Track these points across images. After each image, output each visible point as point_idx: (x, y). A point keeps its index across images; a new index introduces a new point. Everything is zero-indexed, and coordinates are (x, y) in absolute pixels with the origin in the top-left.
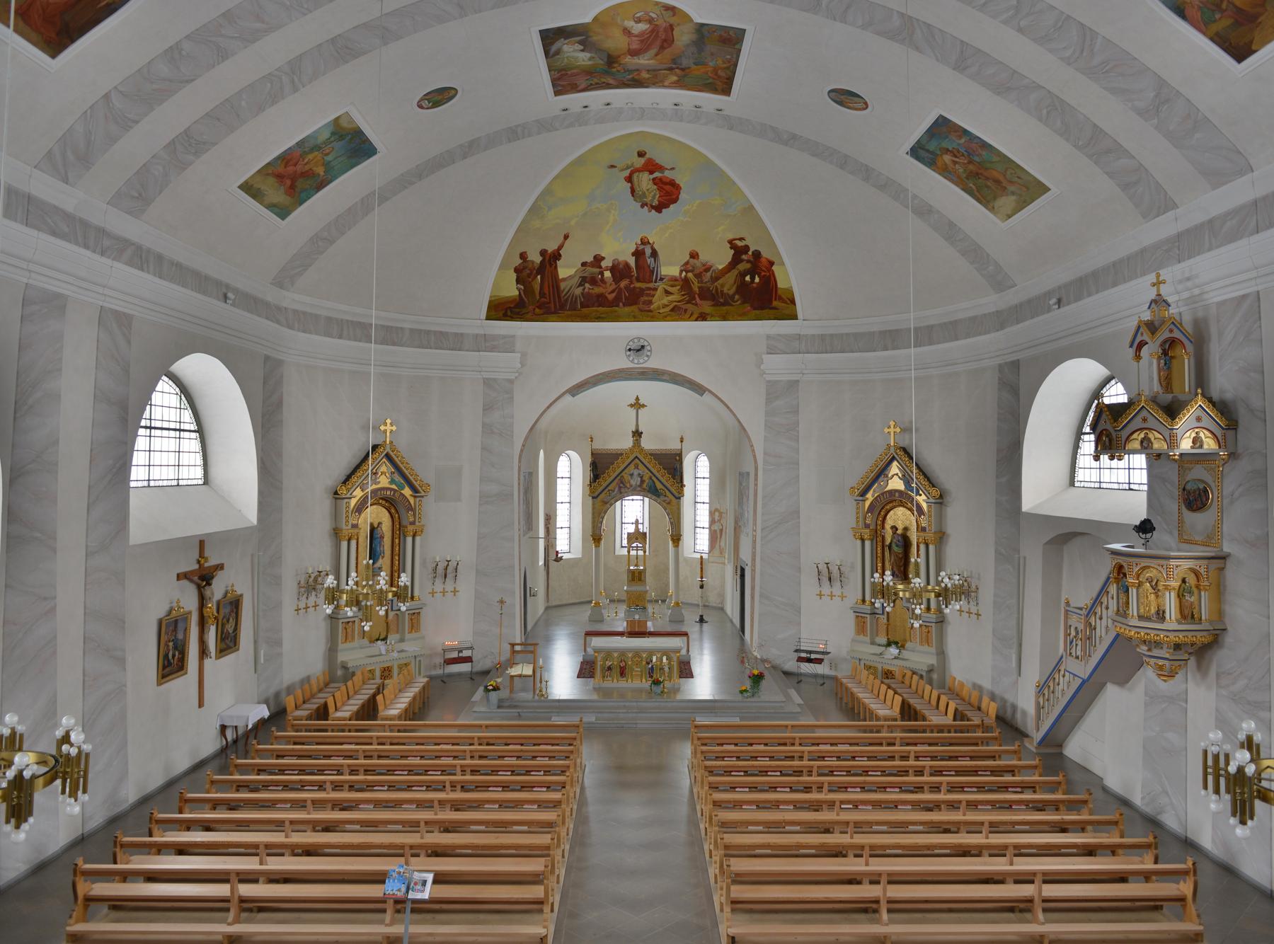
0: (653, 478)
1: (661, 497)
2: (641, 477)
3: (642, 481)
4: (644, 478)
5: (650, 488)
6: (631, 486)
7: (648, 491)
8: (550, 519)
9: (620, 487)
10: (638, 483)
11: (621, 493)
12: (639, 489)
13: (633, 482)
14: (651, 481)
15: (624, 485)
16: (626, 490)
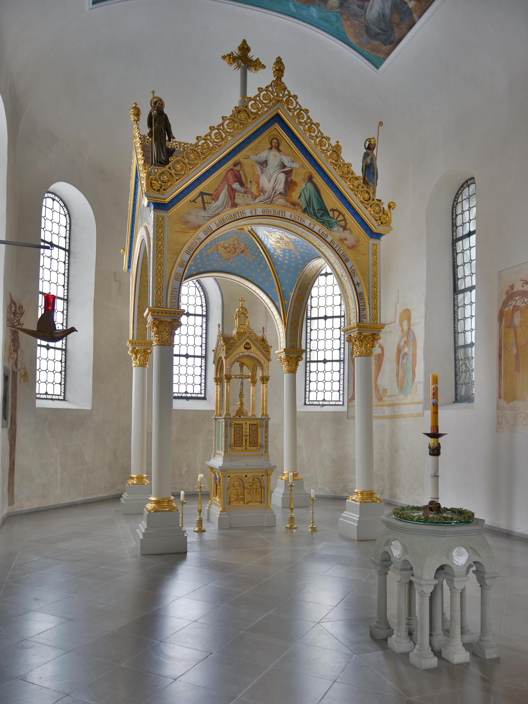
0: (318, 180)
1: (336, 228)
2: (288, 173)
3: (289, 185)
4: (293, 177)
5: (309, 203)
6: (262, 191)
7: (305, 211)
8: (22, 314)
9: (232, 192)
10: (280, 187)
11: (235, 205)
12: (281, 201)
13: (266, 183)
14: (309, 185)
15: (242, 184)
16: (248, 198)
